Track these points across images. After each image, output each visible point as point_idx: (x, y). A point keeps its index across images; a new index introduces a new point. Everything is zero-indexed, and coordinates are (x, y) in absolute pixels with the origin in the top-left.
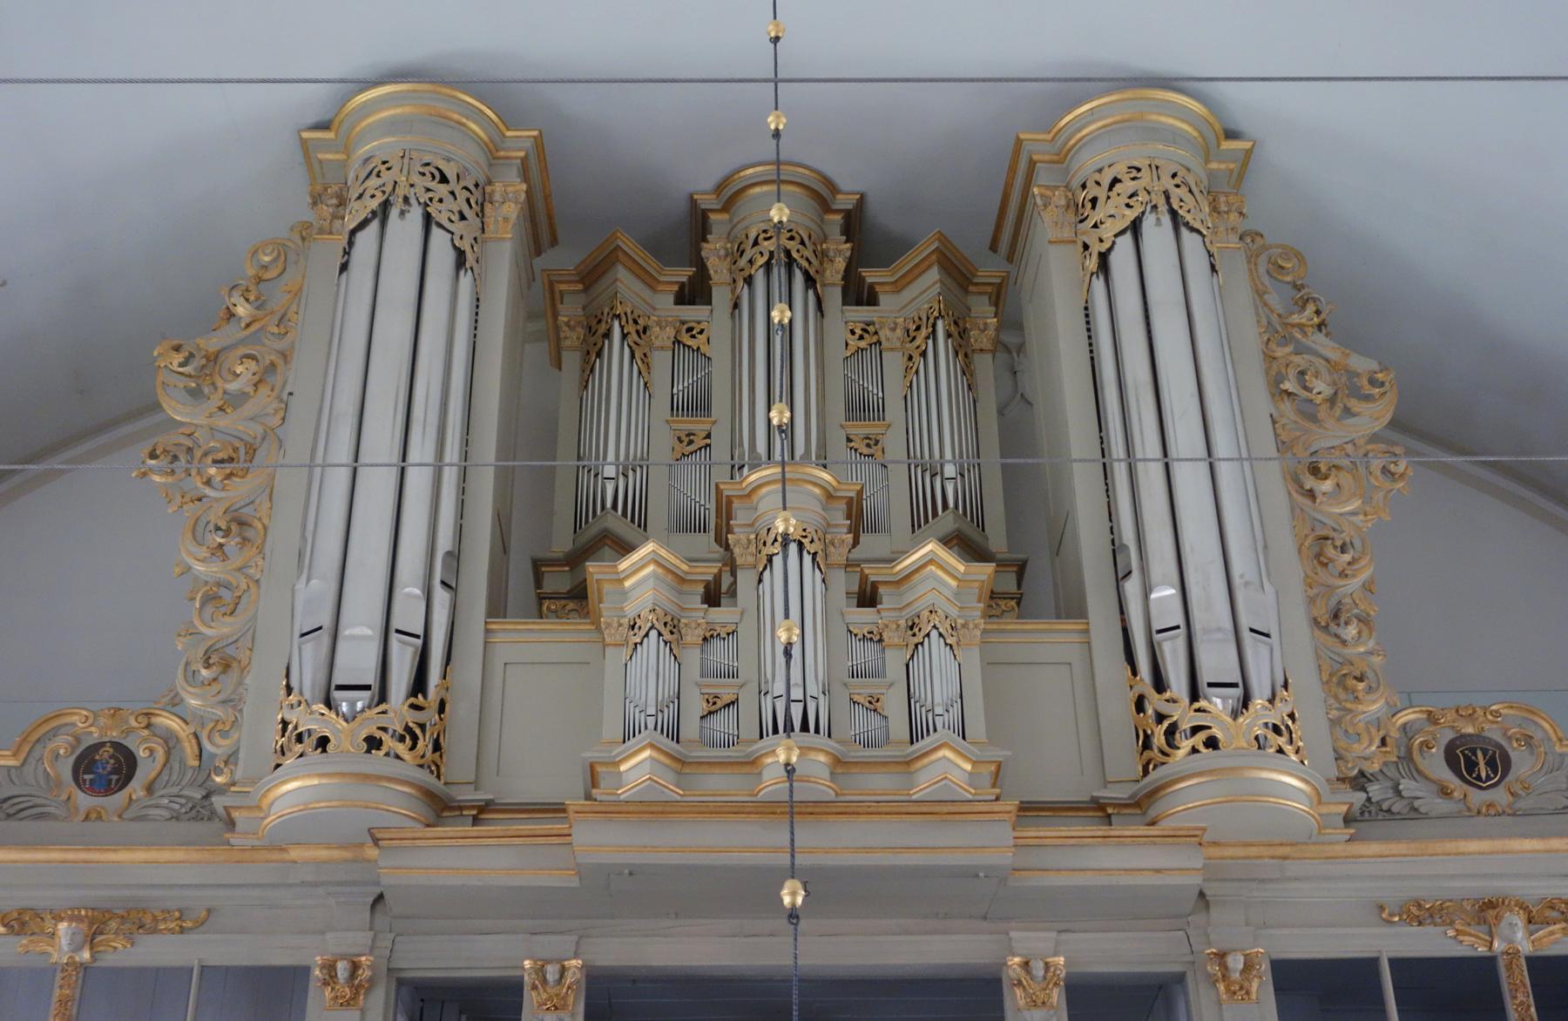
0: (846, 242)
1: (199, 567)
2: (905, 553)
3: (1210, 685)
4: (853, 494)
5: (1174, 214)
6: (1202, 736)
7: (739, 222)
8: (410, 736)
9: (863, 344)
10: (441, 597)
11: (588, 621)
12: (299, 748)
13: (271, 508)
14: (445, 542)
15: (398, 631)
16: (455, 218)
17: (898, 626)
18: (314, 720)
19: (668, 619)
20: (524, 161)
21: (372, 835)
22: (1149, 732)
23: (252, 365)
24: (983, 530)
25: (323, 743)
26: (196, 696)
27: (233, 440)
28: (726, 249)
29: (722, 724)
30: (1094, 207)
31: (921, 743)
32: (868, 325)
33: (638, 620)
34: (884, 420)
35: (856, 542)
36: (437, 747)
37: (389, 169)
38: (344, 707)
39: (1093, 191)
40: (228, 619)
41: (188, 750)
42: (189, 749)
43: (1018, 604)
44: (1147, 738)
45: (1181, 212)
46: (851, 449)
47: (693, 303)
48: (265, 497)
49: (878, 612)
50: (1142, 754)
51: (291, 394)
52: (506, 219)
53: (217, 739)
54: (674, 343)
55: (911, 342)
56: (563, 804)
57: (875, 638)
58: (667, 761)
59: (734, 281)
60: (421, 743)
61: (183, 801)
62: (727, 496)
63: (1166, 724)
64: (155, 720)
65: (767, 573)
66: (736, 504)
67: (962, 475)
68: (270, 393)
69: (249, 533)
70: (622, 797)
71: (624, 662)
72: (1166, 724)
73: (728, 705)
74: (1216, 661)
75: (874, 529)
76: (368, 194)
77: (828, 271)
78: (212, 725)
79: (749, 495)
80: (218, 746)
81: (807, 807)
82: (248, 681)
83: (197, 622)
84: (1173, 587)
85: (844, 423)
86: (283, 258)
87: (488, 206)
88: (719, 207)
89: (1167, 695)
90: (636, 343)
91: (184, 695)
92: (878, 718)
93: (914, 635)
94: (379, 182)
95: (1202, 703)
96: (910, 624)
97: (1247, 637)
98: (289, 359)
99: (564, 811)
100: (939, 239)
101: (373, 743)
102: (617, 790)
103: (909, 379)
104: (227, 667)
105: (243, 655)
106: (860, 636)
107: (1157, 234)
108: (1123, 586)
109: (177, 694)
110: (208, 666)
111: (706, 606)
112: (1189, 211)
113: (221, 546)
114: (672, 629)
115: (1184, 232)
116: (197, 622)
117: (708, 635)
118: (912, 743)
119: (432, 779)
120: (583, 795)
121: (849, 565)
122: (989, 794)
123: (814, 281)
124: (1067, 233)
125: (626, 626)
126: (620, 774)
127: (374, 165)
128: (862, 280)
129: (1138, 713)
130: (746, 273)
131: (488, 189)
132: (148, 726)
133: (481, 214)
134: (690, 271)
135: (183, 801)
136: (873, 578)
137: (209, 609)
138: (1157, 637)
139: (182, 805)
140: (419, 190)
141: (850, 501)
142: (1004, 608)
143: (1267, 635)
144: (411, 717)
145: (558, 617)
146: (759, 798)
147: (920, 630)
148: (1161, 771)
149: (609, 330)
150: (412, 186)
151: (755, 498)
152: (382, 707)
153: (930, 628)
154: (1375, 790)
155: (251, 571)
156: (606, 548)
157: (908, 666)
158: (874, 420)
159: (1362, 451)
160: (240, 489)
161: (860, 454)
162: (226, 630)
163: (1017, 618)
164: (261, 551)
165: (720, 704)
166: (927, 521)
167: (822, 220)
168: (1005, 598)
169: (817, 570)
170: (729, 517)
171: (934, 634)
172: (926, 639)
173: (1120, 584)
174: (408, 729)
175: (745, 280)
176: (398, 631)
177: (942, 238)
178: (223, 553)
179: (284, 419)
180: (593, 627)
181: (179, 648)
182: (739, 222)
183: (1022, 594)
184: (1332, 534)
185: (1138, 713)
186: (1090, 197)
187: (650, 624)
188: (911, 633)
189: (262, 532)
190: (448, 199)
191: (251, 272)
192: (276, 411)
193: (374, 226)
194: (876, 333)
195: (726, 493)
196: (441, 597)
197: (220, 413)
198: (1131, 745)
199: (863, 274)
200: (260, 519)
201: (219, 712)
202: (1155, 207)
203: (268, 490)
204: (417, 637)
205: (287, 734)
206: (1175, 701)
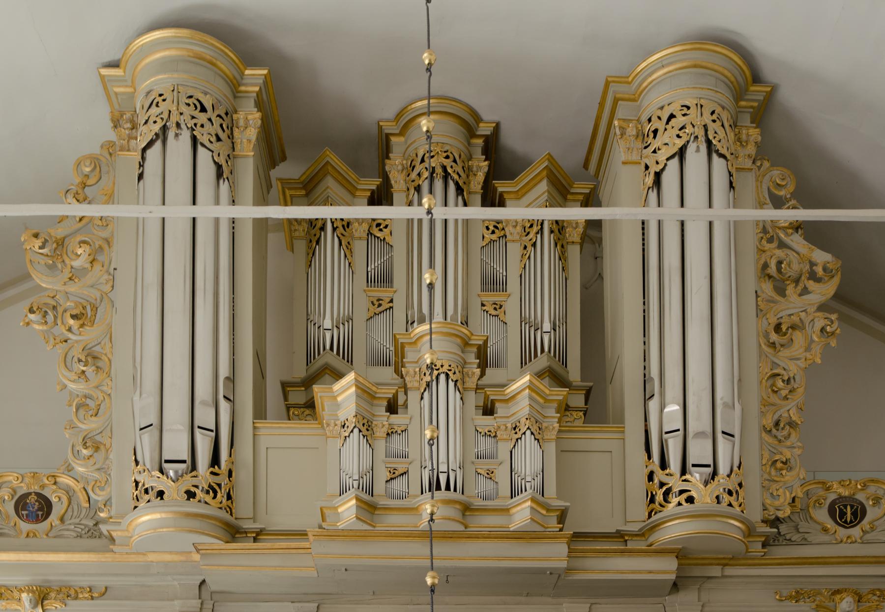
0: (485, 160)
1: (72, 386)
2: (513, 380)
3: (694, 466)
4: (481, 343)
5: (709, 143)
6: (685, 496)
7: (411, 144)
8: (213, 490)
9: (494, 237)
10: (224, 406)
11: (317, 422)
12: (147, 497)
13: (112, 347)
14: (224, 371)
15: (199, 427)
16: (213, 139)
17: (507, 427)
18: (155, 481)
19: (365, 421)
20: (259, 94)
21: (195, 547)
22: (654, 493)
23: (87, 248)
24: (566, 366)
25: (161, 494)
26: (82, 466)
27: (82, 301)
28: (403, 165)
29: (398, 485)
30: (655, 137)
31: (517, 498)
32: (498, 223)
33: (346, 422)
34: (506, 291)
35: (483, 374)
36: (229, 497)
37: (164, 100)
38: (171, 473)
39: (656, 124)
40: (93, 418)
41: (81, 497)
42: (82, 497)
43: (585, 415)
44: (653, 497)
45: (714, 142)
46: (484, 311)
47: (381, 205)
48: (107, 339)
49: (495, 418)
50: (649, 506)
51: (115, 269)
52: (249, 141)
53: (97, 490)
54: (368, 235)
55: (526, 236)
56: (306, 531)
57: (492, 435)
58: (366, 507)
59: (408, 189)
60: (219, 495)
61: (83, 527)
62: (401, 343)
63: (664, 488)
64: (58, 479)
65: (426, 394)
66: (407, 349)
67: (555, 330)
68: (101, 268)
69: (100, 364)
70: (340, 527)
71: (339, 448)
72: (664, 488)
73: (402, 474)
74: (699, 451)
75: (497, 365)
76: (151, 121)
77: (472, 182)
78: (93, 483)
79: (415, 343)
80: (99, 496)
81: (448, 534)
82: (111, 456)
83: (76, 421)
84: (679, 405)
85: (480, 293)
86: (98, 168)
87: (236, 132)
88: (397, 131)
89: (667, 471)
90: (342, 234)
91: (74, 465)
92: (492, 482)
93: (516, 433)
94: (158, 110)
95: (688, 477)
96: (514, 426)
97: (720, 436)
98: (111, 245)
99: (306, 535)
100: (548, 159)
101: (190, 495)
102: (337, 523)
103: (523, 262)
104: (97, 449)
105: (107, 441)
106: (483, 433)
107: (696, 158)
108: (648, 404)
109: (70, 464)
110: (86, 448)
111: (388, 414)
112: (719, 141)
113: (83, 372)
114: (366, 427)
115: (715, 156)
116: (76, 421)
117: (390, 432)
118: (512, 498)
119: (227, 516)
120: (317, 526)
121: (478, 388)
122: (557, 527)
123: (462, 190)
124: (635, 157)
125: (340, 426)
126: (338, 514)
127: (153, 97)
128: (495, 189)
129: (649, 482)
130: (416, 184)
131: (235, 116)
132: (55, 483)
133: (231, 137)
134: (378, 181)
135: (83, 527)
136: (492, 397)
137: (82, 412)
138: (665, 436)
139: (82, 529)
140: (187, 117)
141: (479, 347)
142: (576, 417)
143: (732, 436)
144: (212, 480)
145: (300, 419)
146: (420, 528)
147: (520, 430)
148: (659, 516)
149: (324, 225)
150: (181, 114)
151: (419, 345)
152: (194, 473)
153: (526, 429)
154: (783, 528)
155: (105, 388)
156: (327, 375)
157: (511, 452)
158: (500, 291)
159: (811, 318)
160: (90, 334)
161: (490, 315)
162: (93, 426)
163: (583, 423)
164: (109, 375)
165: (397, 473)
166: (530, 360)
167: (469, 144)
168: (576, 411)
169: (457, 392)
170: (403, 357)
171: (528, 433)
172: (523, 436)
173: (647, 402)
174: (210, 486)
175: (415, 188)
176: (199, 427)
177: (550, 158)
178: (86, 376)
179: (113, 287)
180: (320, 426)
181: (67, 436)
182: (411, 144)
183: (587, 408)
184: (782, 372)
185: (649, 482)
186: (653, 129)
187: (353, 425)
188: (514, 432)
189: (108, 363)
190: (208, 125)
191: (78, 180)
192: (107, 281)
193: (158, 144)
194: (503, 229)
195: (400, 341)
196: (224, 406)
197: (71, 282)
198: (643, 501)
199: (496, 185)
200: (106, 355)
201: (96, 475)
202: (696, 137)
203: (108, 336)
204: (212, 431)
205: (139, 489)
206: (671, 475)
